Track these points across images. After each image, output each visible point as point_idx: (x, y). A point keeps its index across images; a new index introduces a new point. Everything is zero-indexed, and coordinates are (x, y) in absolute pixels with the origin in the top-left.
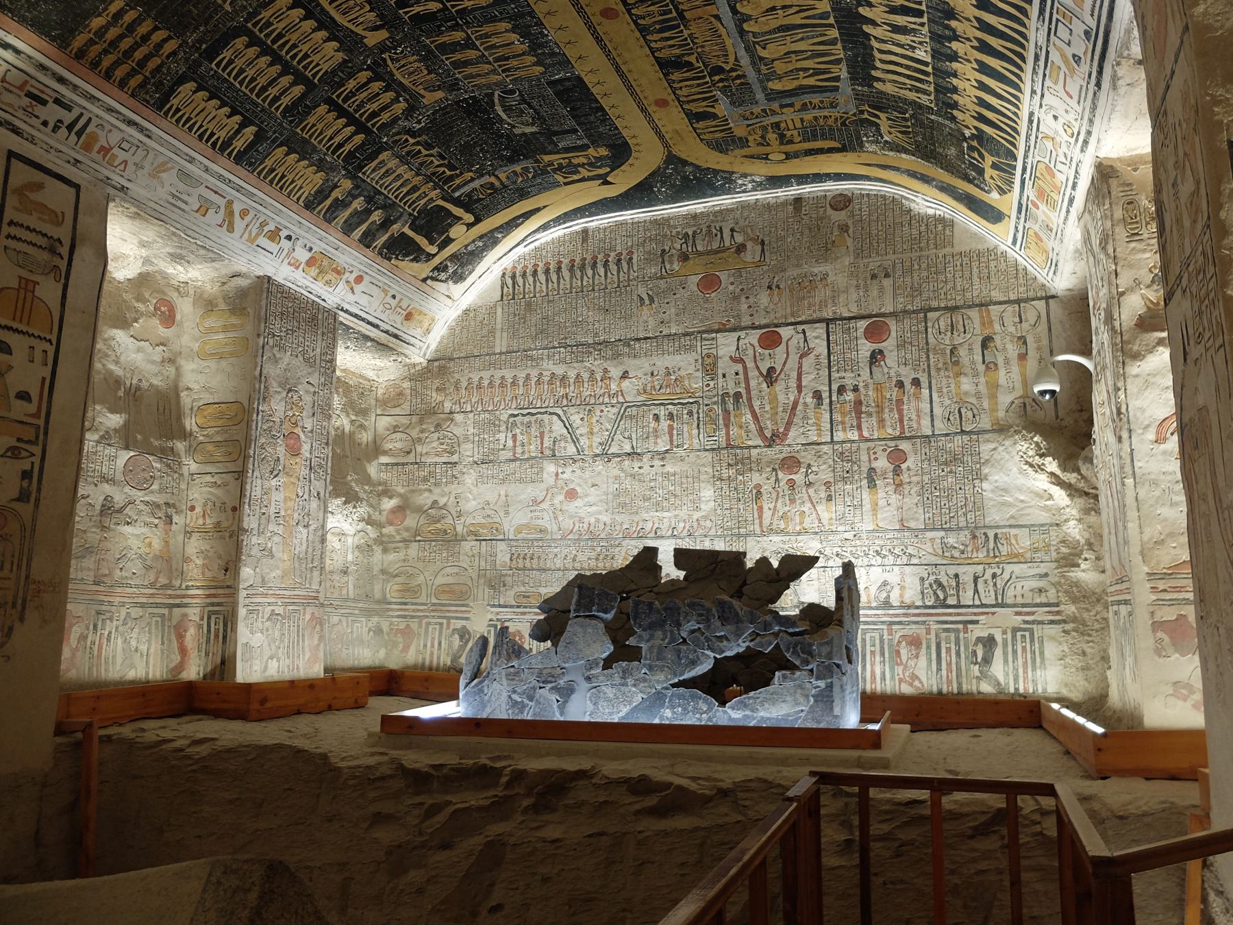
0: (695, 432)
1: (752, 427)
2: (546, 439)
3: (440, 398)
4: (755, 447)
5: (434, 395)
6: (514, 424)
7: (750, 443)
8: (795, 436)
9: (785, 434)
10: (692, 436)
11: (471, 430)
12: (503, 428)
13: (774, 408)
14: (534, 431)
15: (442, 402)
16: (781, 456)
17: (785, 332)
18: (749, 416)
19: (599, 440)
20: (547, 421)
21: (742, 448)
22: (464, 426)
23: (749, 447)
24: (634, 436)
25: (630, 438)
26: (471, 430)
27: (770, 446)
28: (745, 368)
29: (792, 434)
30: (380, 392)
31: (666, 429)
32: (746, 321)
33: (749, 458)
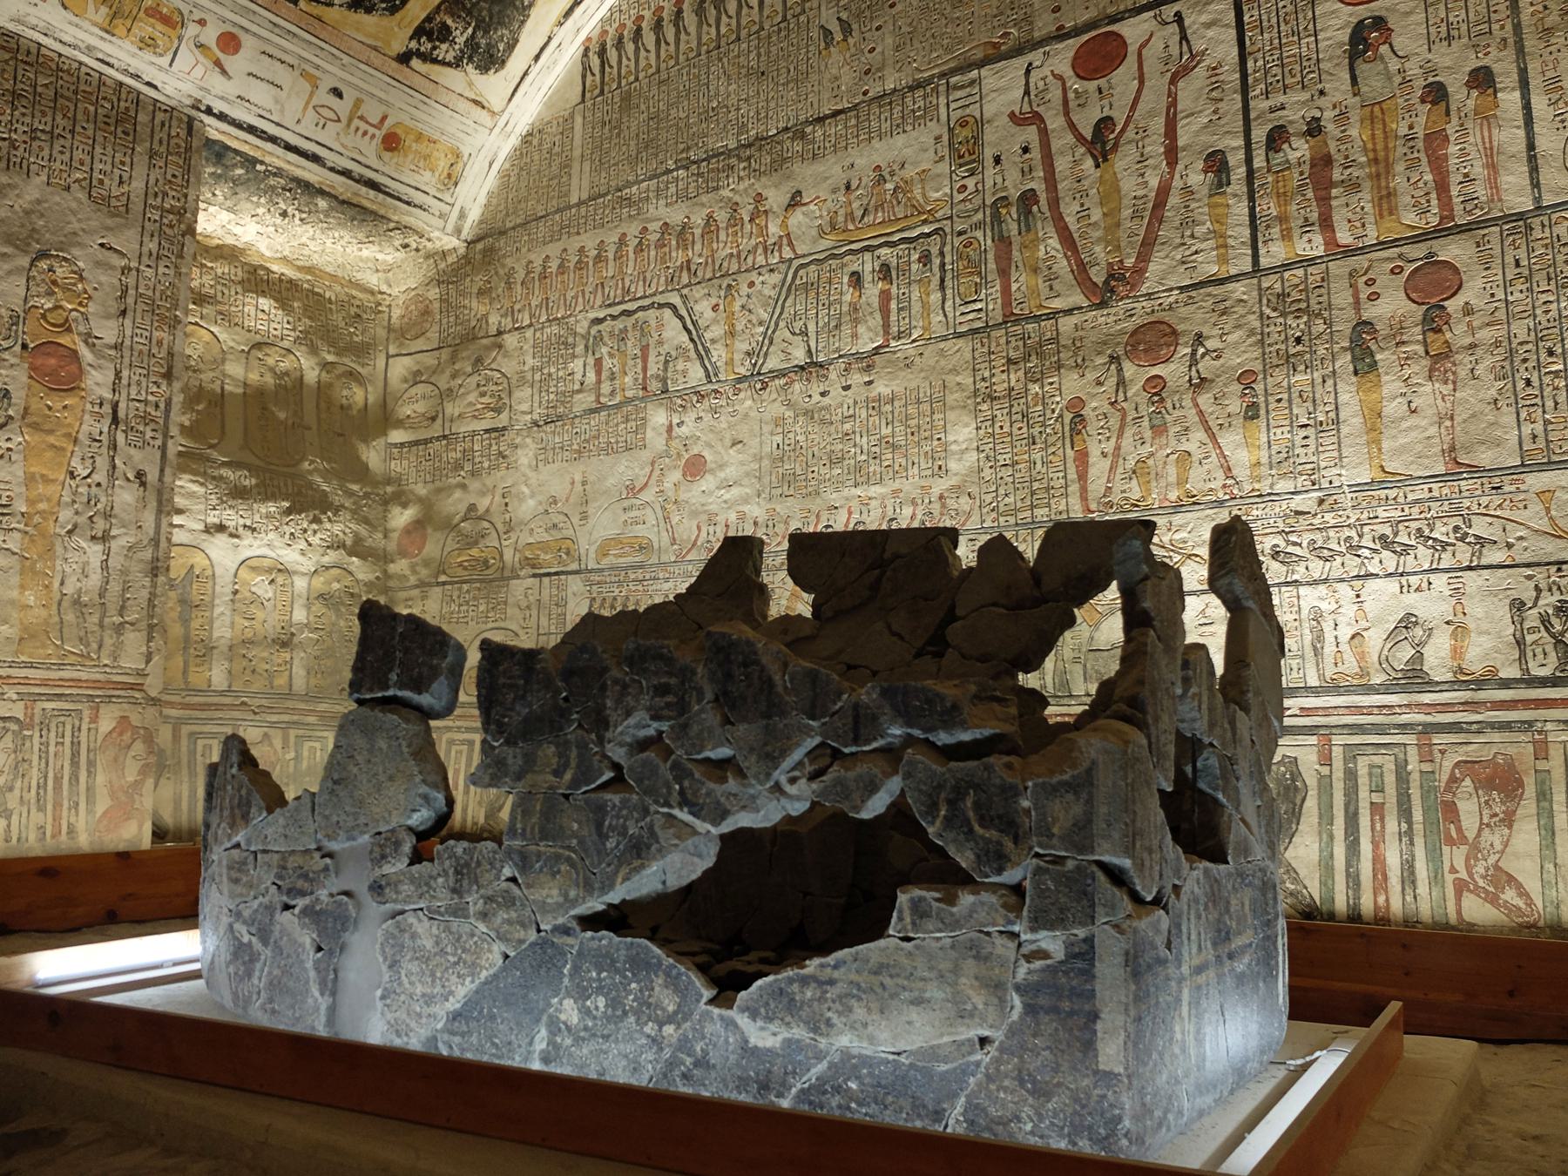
0: (936, 297)
1: (1062, 265)
2: (652, 358)
3: (483, 310)
4: (1069, 312)
5: (474, 304)
6: (599, 338)
7: (1057, 304)
8: (1163, 273)
9: (1139, 271)
10: (930, 308)
11: (530, 362)
12: (580, 349)
13: (1111, 214)
14: (632, 347)
15: (485, 316)
16: (1129, 325)
17: (1133, 30)
18: (1054, 242)
19: (745, 347)
20: (653, 323)
21: (1037, 319)
22: (519, 355)
23: (1054, 315)
24: (812, 328)
25: (804, 333)
26: (530, 362)
27: (1103, 304)
28: (1044, 133)
29: (1154, 268)
30: (396, 313)
31: (875, 302)
32: (1044, 25)
33: (1055, 340)
